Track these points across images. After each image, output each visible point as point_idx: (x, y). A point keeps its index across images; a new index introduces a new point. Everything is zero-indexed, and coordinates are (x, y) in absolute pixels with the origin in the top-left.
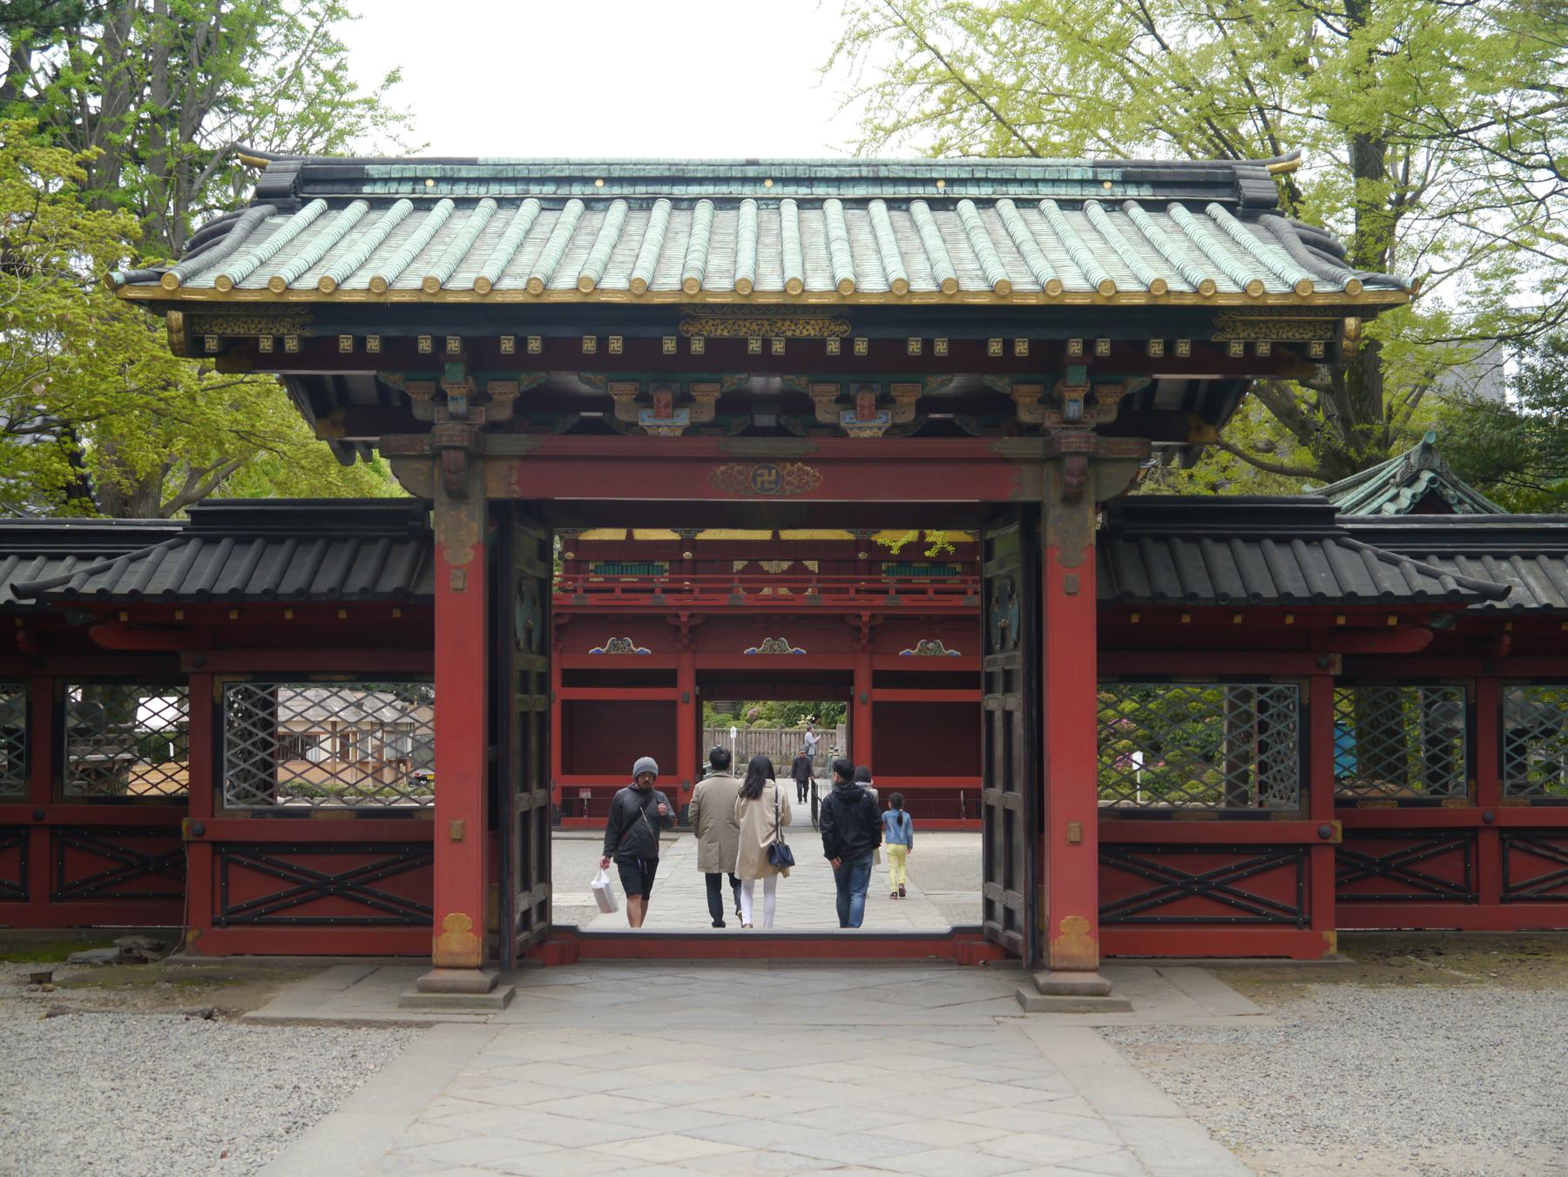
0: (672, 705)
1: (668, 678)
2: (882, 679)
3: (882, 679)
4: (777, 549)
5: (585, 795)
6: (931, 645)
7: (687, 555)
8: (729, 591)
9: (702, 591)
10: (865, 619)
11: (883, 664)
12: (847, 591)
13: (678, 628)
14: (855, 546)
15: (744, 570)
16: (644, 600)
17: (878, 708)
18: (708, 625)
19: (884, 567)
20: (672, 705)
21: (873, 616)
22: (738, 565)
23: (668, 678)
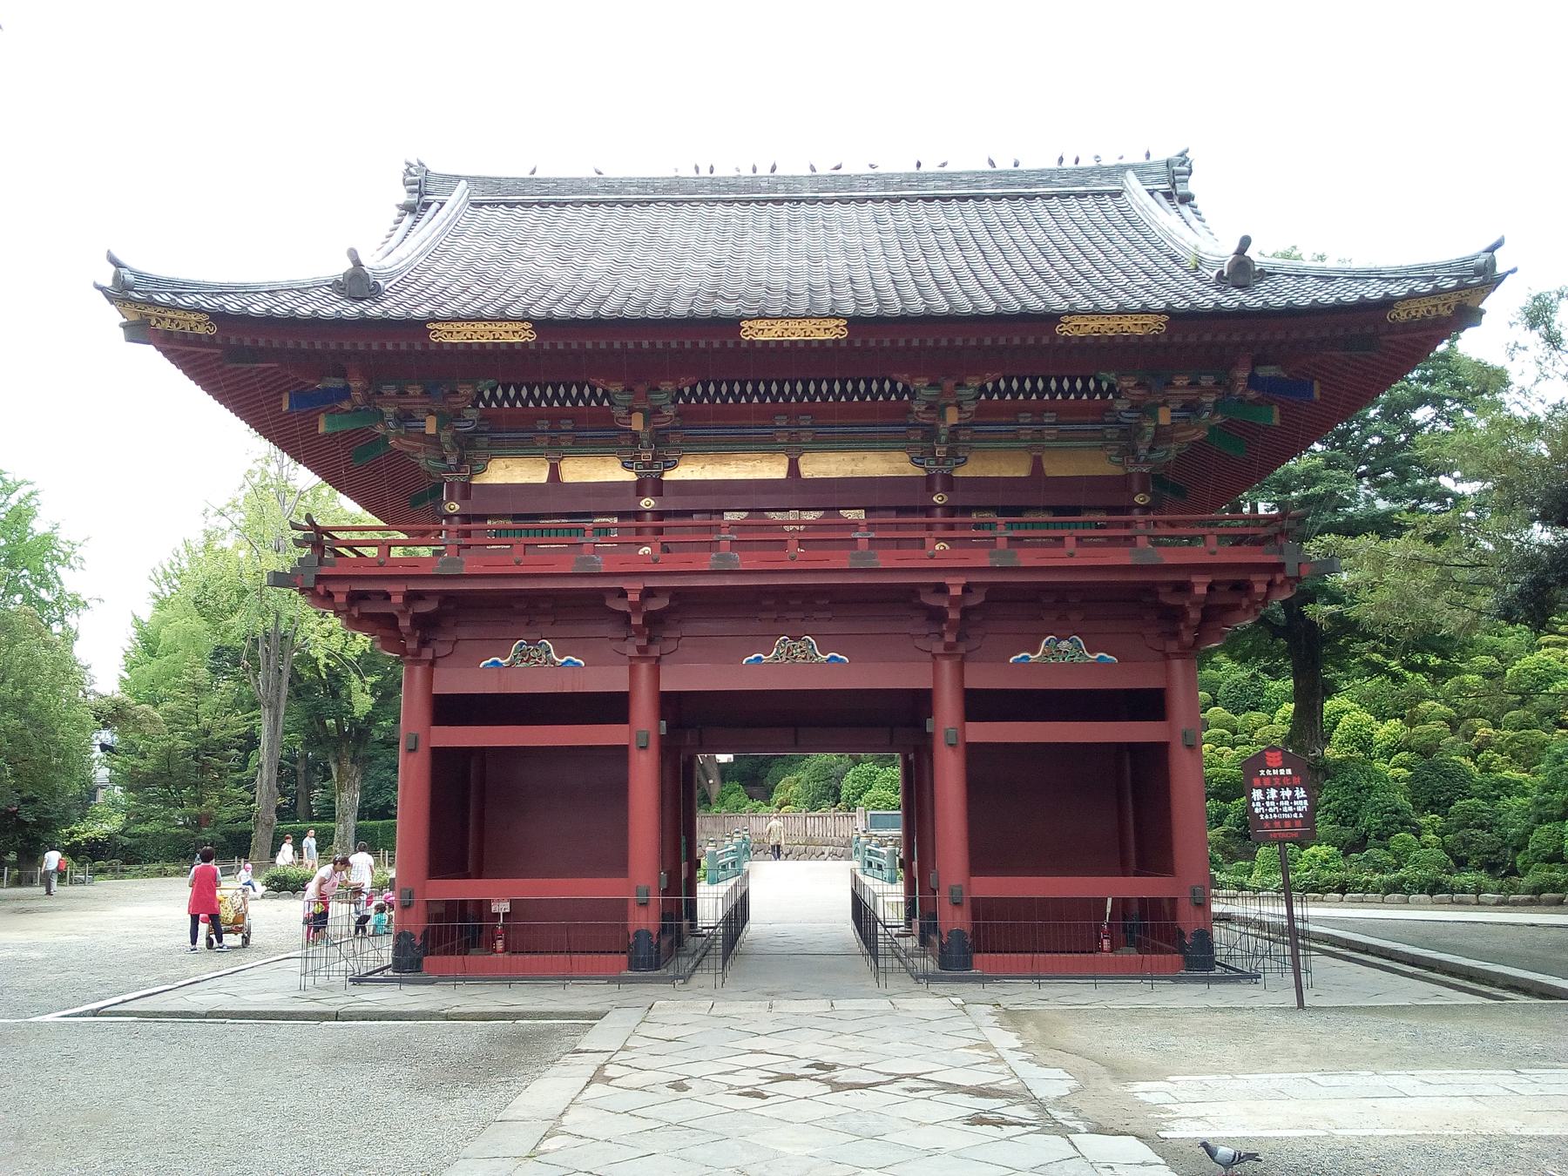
0: (620, 754)
2: (979, 705)
3: (979, 705)
4: (795, 489)
5: (501, 907)
6: (1064, 644)
7: (647, 503)
8: (712, 546)
9: (665, 549)
10: (956, 591)
11: (983, 677)
13: (626, 617)
17: (975, 754)
18: (676, 611)
20: (620, 754)
21: (967, 589)
23: (613, 707)
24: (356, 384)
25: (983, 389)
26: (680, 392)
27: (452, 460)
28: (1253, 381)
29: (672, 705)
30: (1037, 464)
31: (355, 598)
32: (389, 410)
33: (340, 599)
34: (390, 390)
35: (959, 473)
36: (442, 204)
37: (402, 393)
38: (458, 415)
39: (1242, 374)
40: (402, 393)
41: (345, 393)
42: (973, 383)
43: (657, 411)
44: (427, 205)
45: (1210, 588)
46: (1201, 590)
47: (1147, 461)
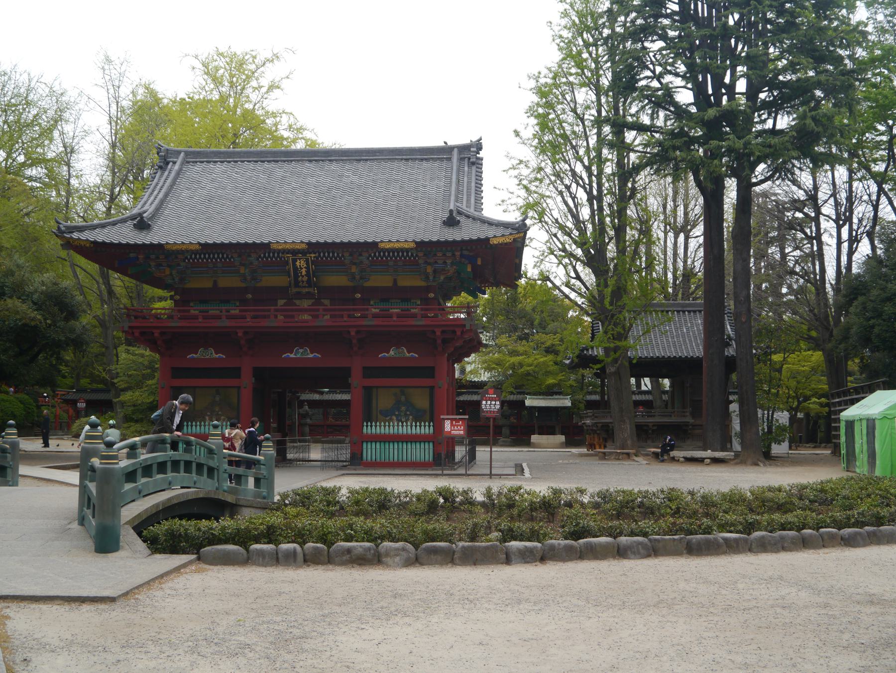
1: (235, 372)
2: (369, 372)
3: (369, 372)
12: (342, 316)
14: (355, 289)
15: (285, 304)
16: (219, 323)
19: (372, 302)
22: (281, 302)
24: (141, 257)
25: (370, 255)
26: (260, 256)
27: (177, 280)
28: (462, 256)
29: (258, 373)
30: (395, 281)
31: (142, 334)
32: (153, 264)
33: (137, 334)
34: (153, 257)
35: (367, 284)
36: (174, 163)
37: (158, 258)
38: (179, 265)
39: (458, 254)
40: (158, 258)
41: (138, 258)
42: (366, 255)
43: (251, 263)
44: (168, 163)
45: (443, 332)
46: (438, 333)
47: (434, 281)
